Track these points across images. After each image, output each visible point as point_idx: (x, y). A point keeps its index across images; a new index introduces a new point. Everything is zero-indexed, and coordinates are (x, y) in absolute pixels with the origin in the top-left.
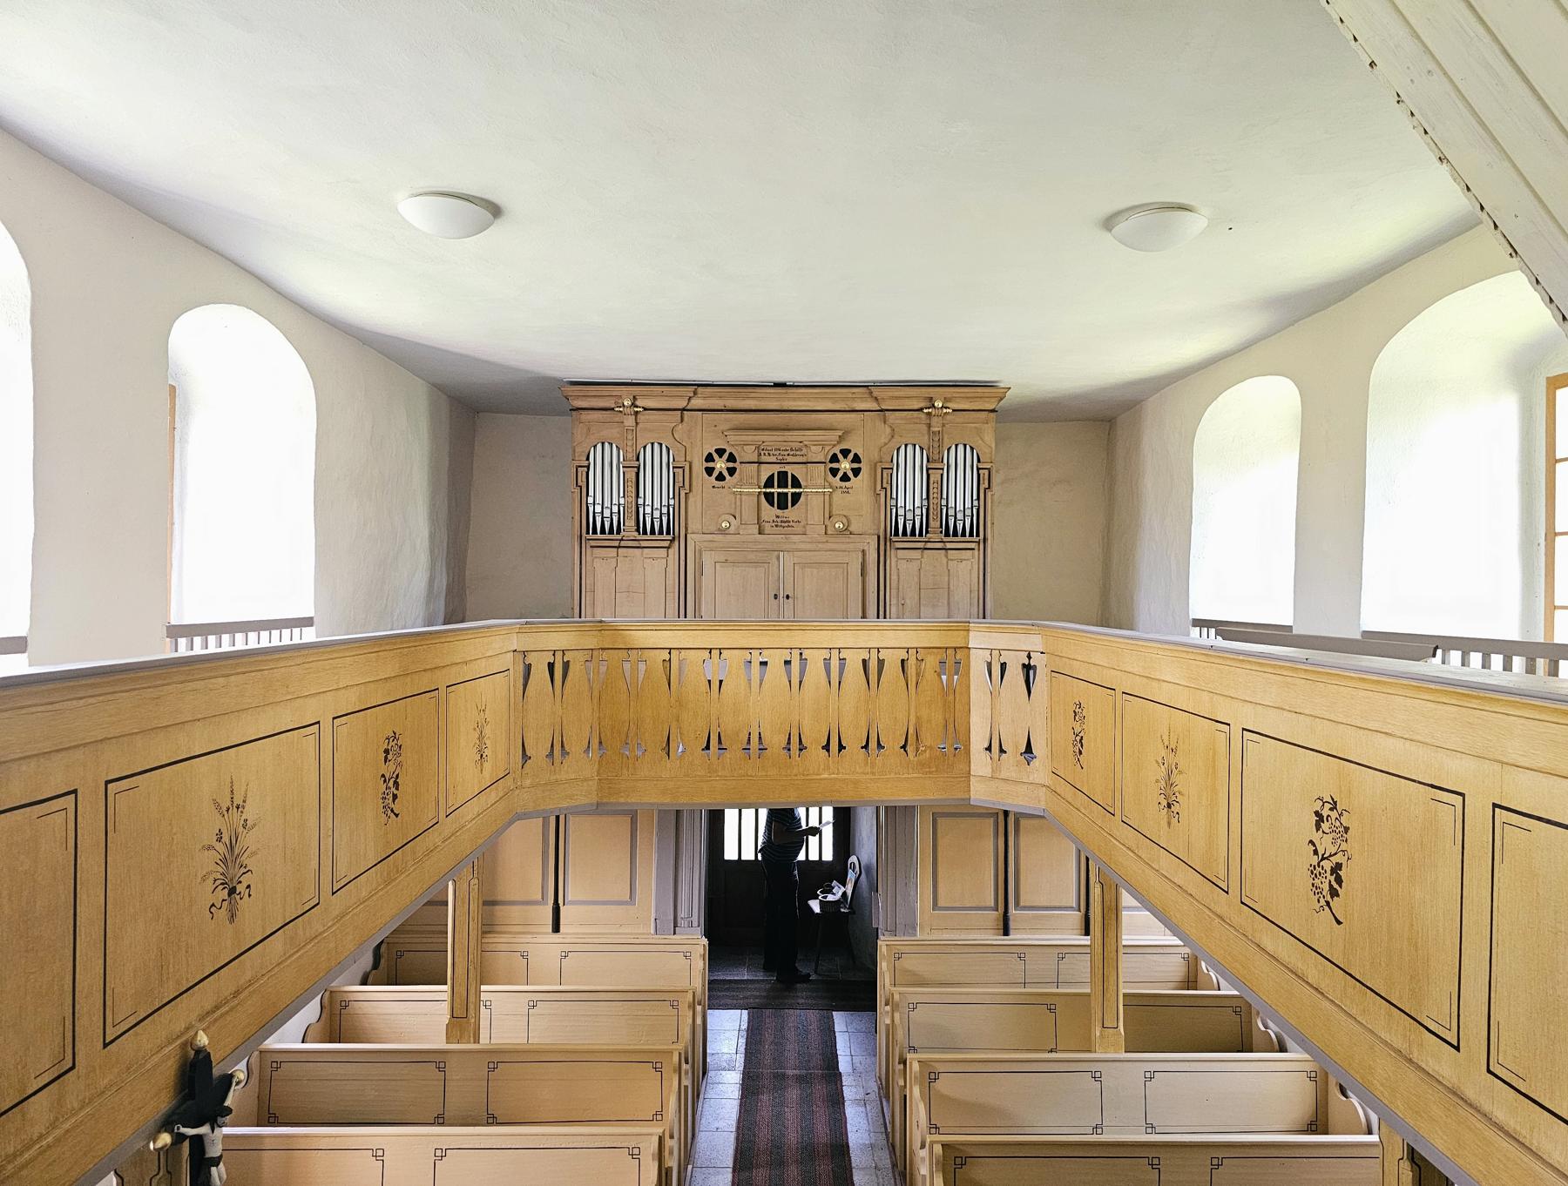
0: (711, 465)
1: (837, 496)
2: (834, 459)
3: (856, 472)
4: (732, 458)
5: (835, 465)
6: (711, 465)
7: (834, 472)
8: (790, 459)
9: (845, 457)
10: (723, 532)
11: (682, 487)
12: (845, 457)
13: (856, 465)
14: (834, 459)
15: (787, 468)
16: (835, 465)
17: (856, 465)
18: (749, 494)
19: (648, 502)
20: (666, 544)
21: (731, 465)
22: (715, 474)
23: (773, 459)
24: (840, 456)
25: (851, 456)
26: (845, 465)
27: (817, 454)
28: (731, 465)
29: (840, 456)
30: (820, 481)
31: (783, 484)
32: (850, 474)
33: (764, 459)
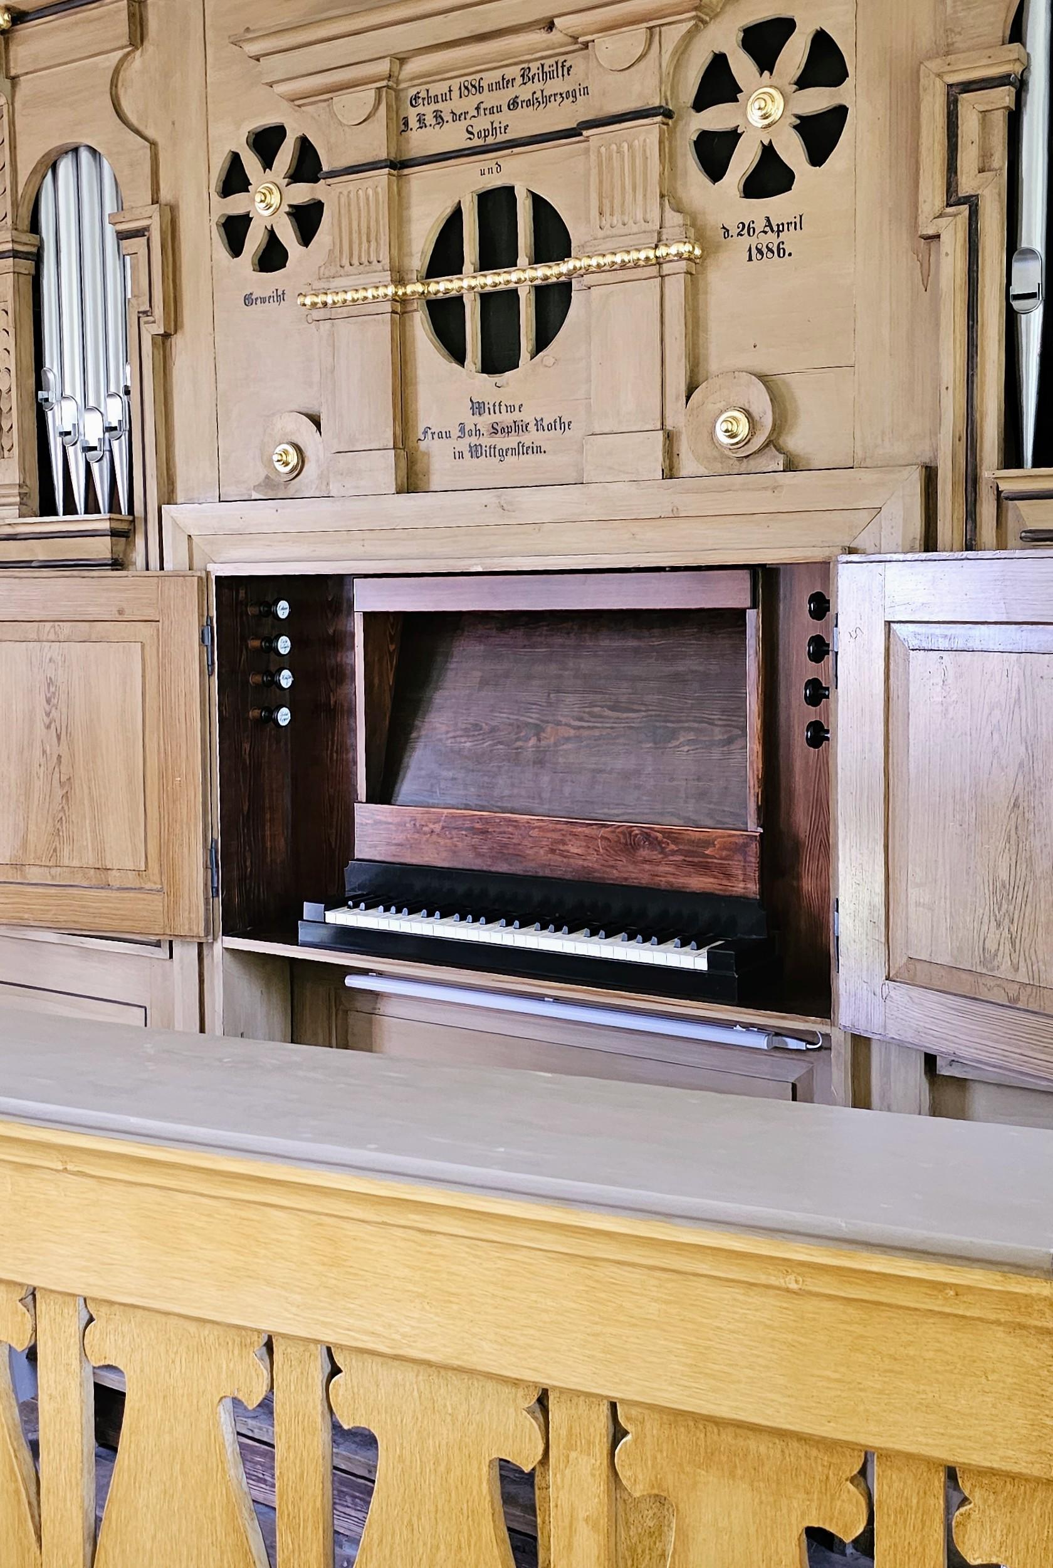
0: (236, 205)
1: (730, 278)
2: (718, 85)
3: (821, 134)
4: (307, 166)
5: (717, 118)
6: (236, 205)
7: (714, 152)
8: (523, 123)
9: (766, 60)
10: (274, 490)
11: (159, 331)
12: (766, 60)
13: (817, 100)
14: (718, 85)
15: (520, 173)
16: (717, 118)
17: (817, 100)
18: (356, 311)
19: (73, 385)
20: (102, 548)
21: (302, 193)
22: (254, 241)
23: (453, 137)
24: (742, 66)
25: (794, 54)
26: (765, 109)
27: (624, 71)
28: (302, 193)
29: (742, 66)
30: (645, 210)
31: (496, 254)
32: (792, 151)
33: (421, 141)
